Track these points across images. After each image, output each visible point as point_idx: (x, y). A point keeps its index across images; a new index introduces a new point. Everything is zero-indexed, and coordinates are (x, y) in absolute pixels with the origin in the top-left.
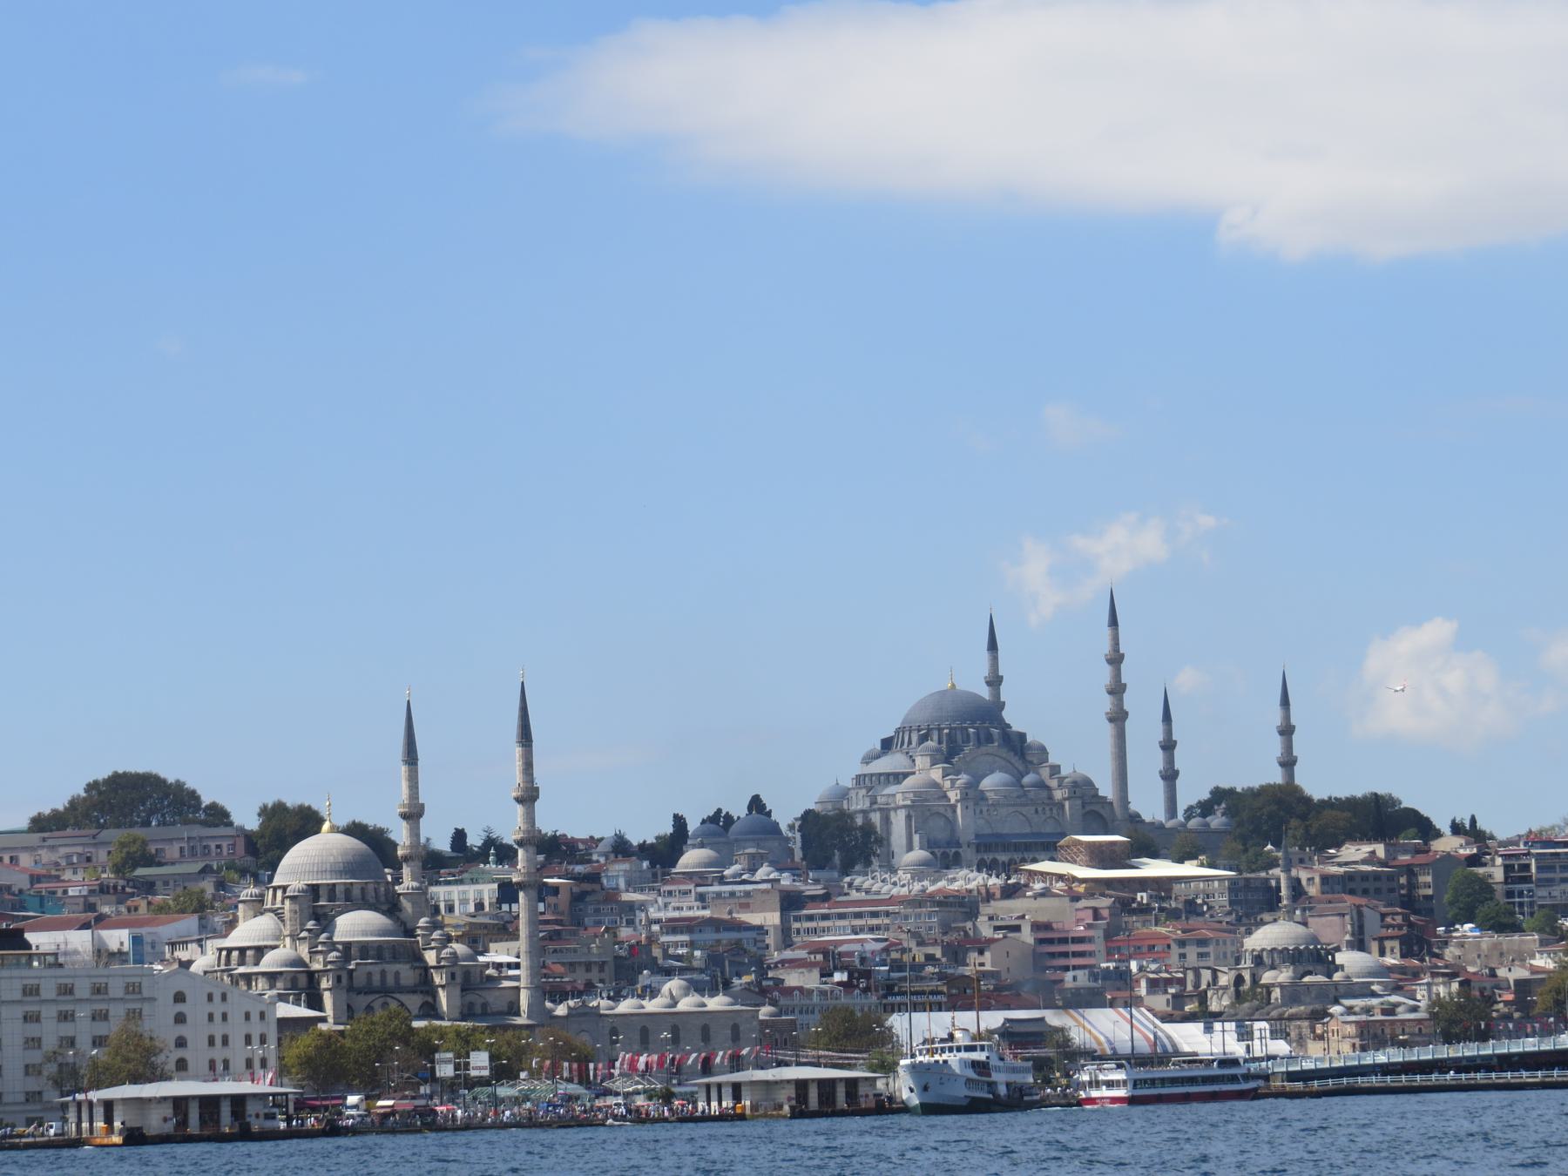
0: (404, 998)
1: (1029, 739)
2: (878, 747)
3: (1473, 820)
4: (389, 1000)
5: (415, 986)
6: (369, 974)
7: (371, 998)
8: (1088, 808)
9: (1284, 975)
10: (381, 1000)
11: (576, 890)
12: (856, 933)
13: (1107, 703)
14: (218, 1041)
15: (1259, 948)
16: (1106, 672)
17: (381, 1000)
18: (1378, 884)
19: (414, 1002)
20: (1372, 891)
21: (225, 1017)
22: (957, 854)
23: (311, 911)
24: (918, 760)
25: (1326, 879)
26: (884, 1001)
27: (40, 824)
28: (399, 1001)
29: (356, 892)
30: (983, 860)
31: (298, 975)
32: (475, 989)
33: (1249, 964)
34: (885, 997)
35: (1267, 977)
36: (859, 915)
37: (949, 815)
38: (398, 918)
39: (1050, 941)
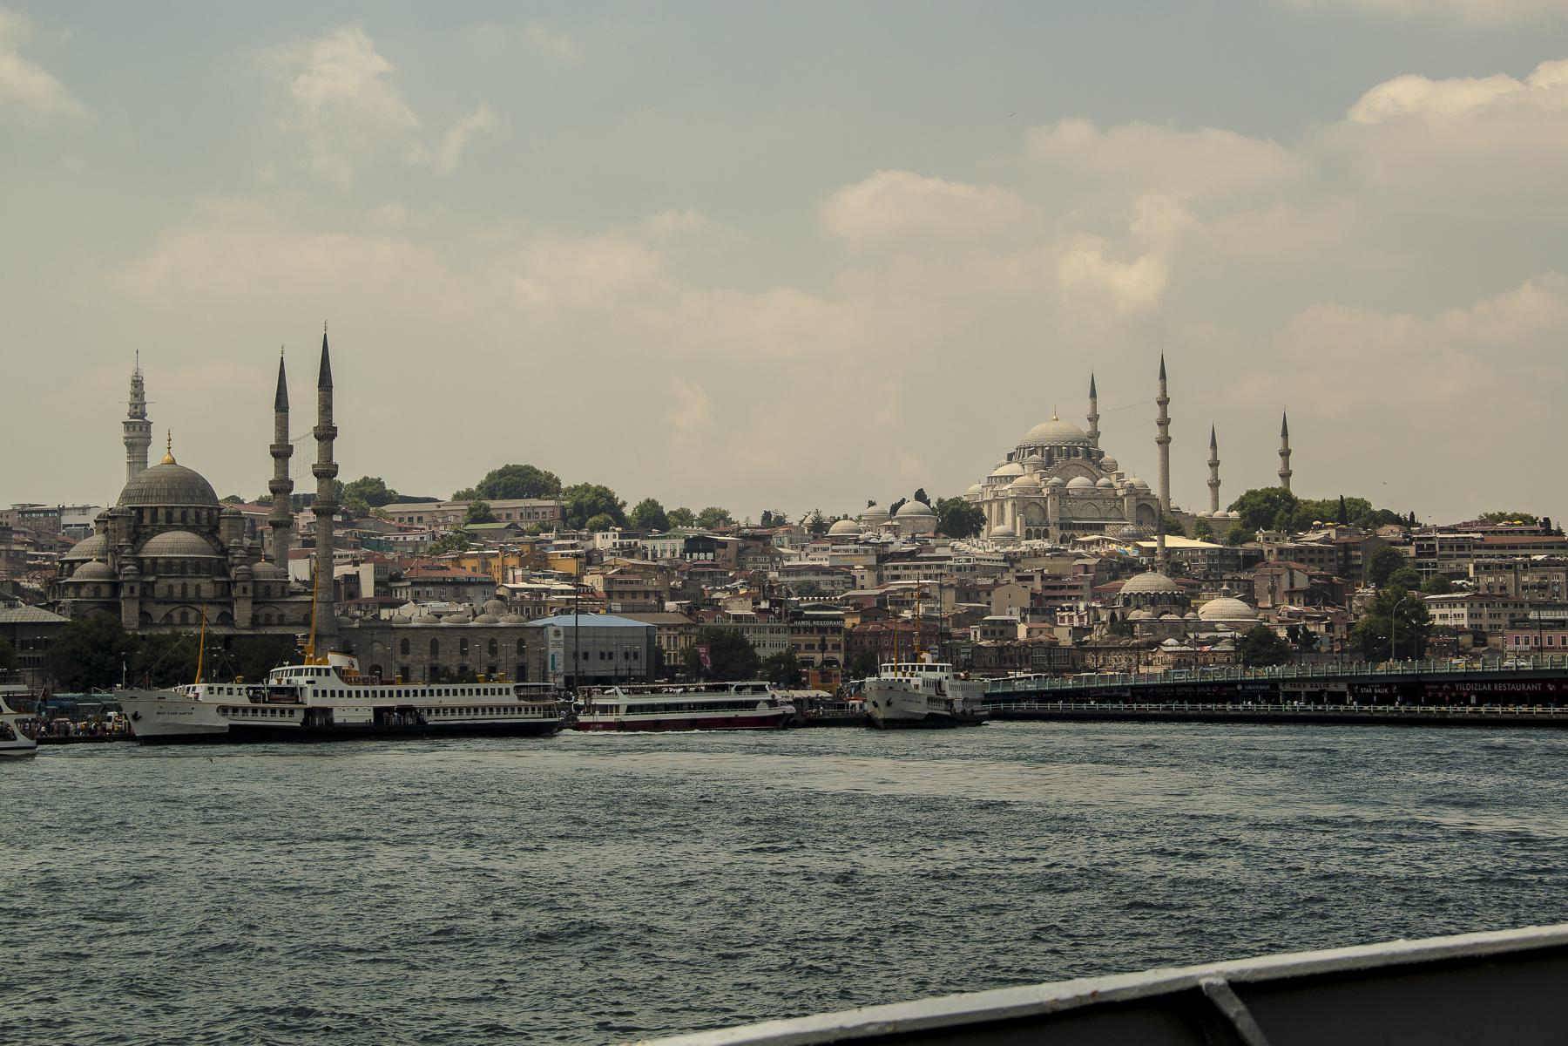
0: (203, 608)
3: (1412, 515)
4: (188, 610)
5: (215, 598)
6: (171, 587)
7: (169, 608)
8: (1141, 502)
9: (1143, 614)
11: (741, 545)
17: (181, 609)
18: (1321, 556)
19: (212, 613)
20: (1316, 560)
22: (1046, 531)
23: (131, 530)
25: (1281, 551)
26: (791, 625)
27: (457, 497)
29: (177, 515)
30: (1064, 535)
31: (102, 586)
33: (1121, 605)
34: (792, 621)
35: (1134, 615)
36: (928, 567)
37: (1042, 504)
39: (1054, 588)
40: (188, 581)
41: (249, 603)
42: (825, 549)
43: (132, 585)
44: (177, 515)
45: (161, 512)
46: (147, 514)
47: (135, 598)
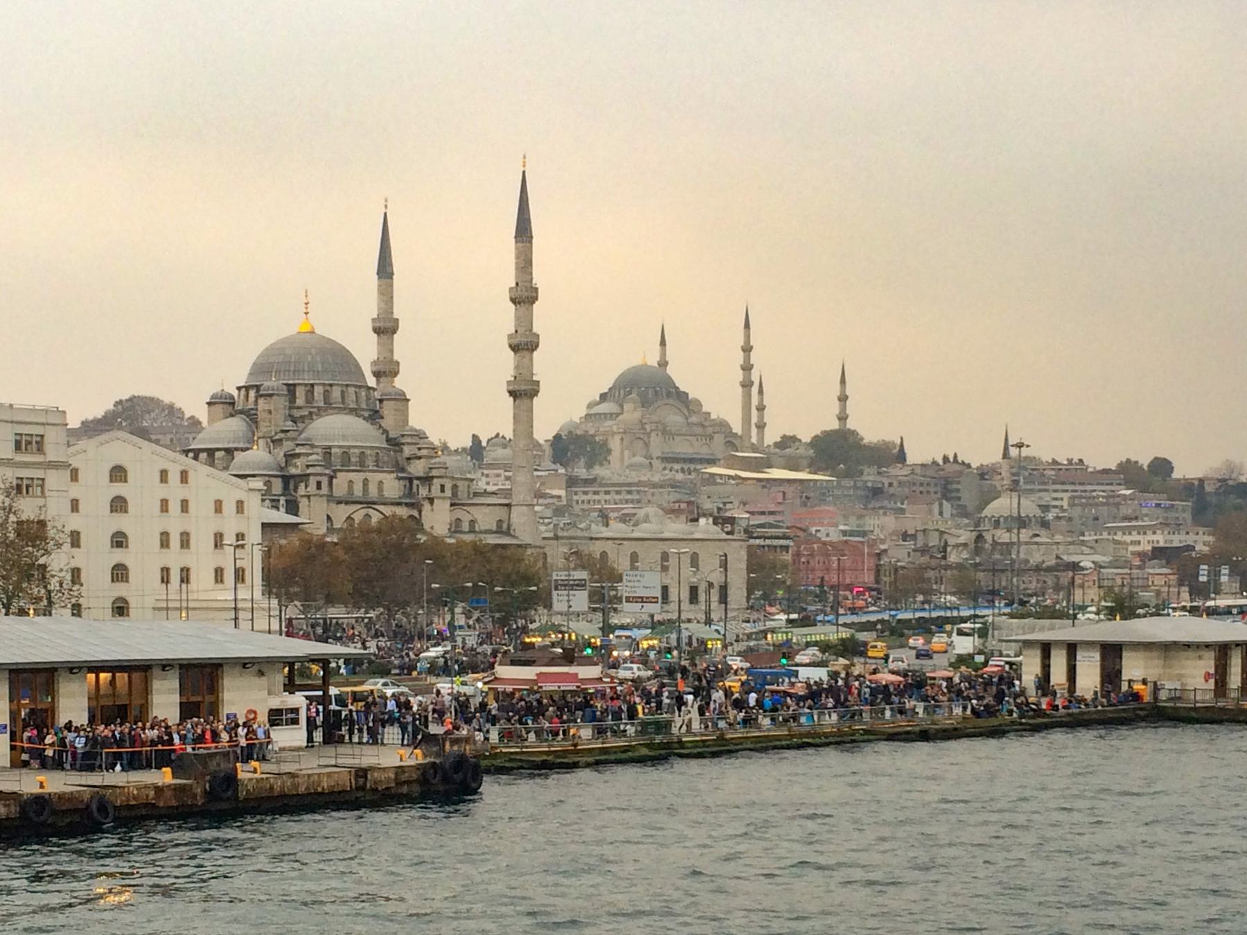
1: (690, 397)
2: (598, 399)
4: (370, 510)
5: (400, 498)
8: (728, 439)
10: (363, 512)
12: (616, 504)
13: (739, 375)
14: (175, 541)
15: (997, 515)
16: (740, 355)
17: (363, 512)
21: (185, 506)
23: (287, 412)
24: (626, 407)
28: (381, 513)
29: (336, 393)
31: (272, 479)
32: (463, 505)
38: (380, 426)
40: (369, 475)
41: (448, 502)
42: (498, 476)
43: (319, 478)
44: (336, 393)
45: (318, 391)
46: (300, 393)
47: (321, 496)
